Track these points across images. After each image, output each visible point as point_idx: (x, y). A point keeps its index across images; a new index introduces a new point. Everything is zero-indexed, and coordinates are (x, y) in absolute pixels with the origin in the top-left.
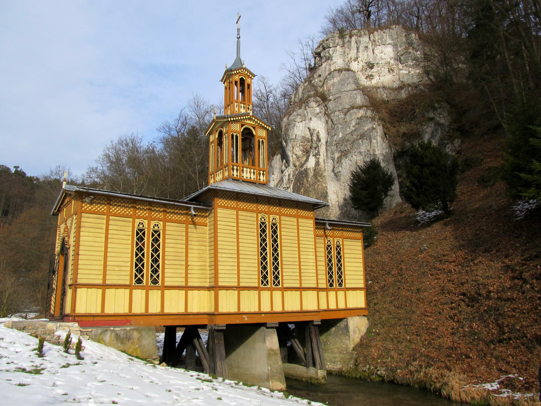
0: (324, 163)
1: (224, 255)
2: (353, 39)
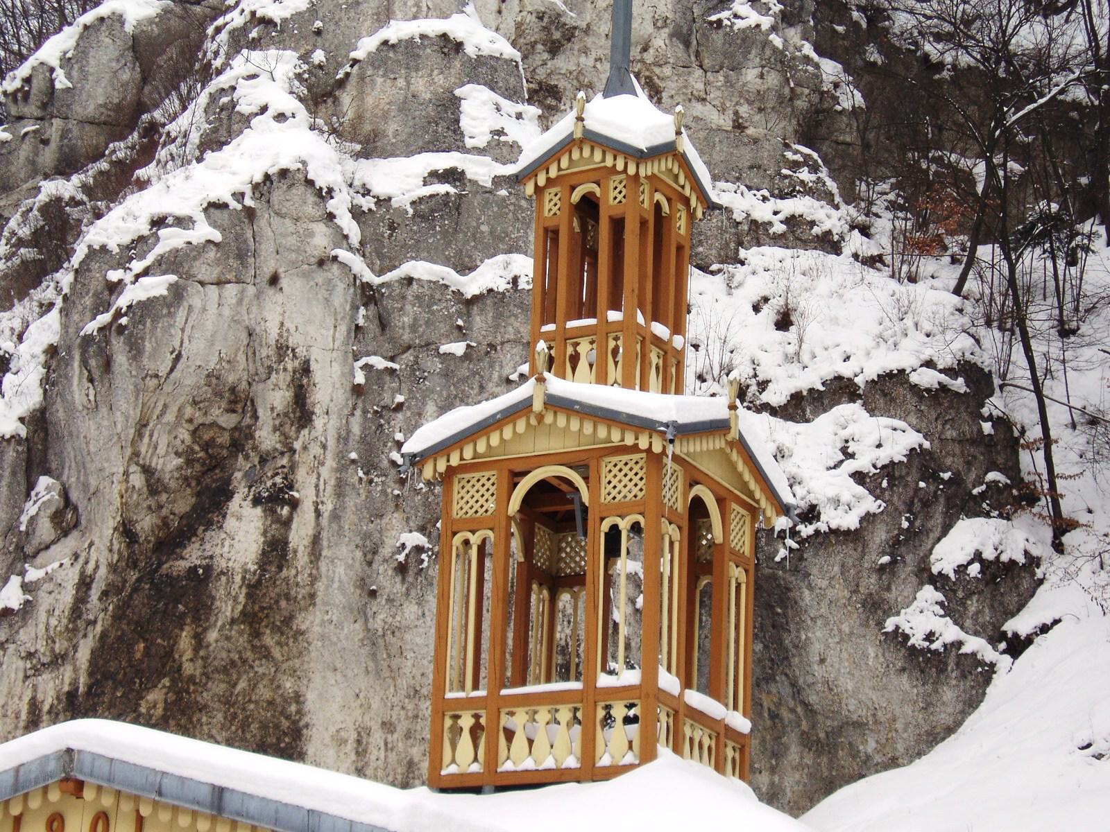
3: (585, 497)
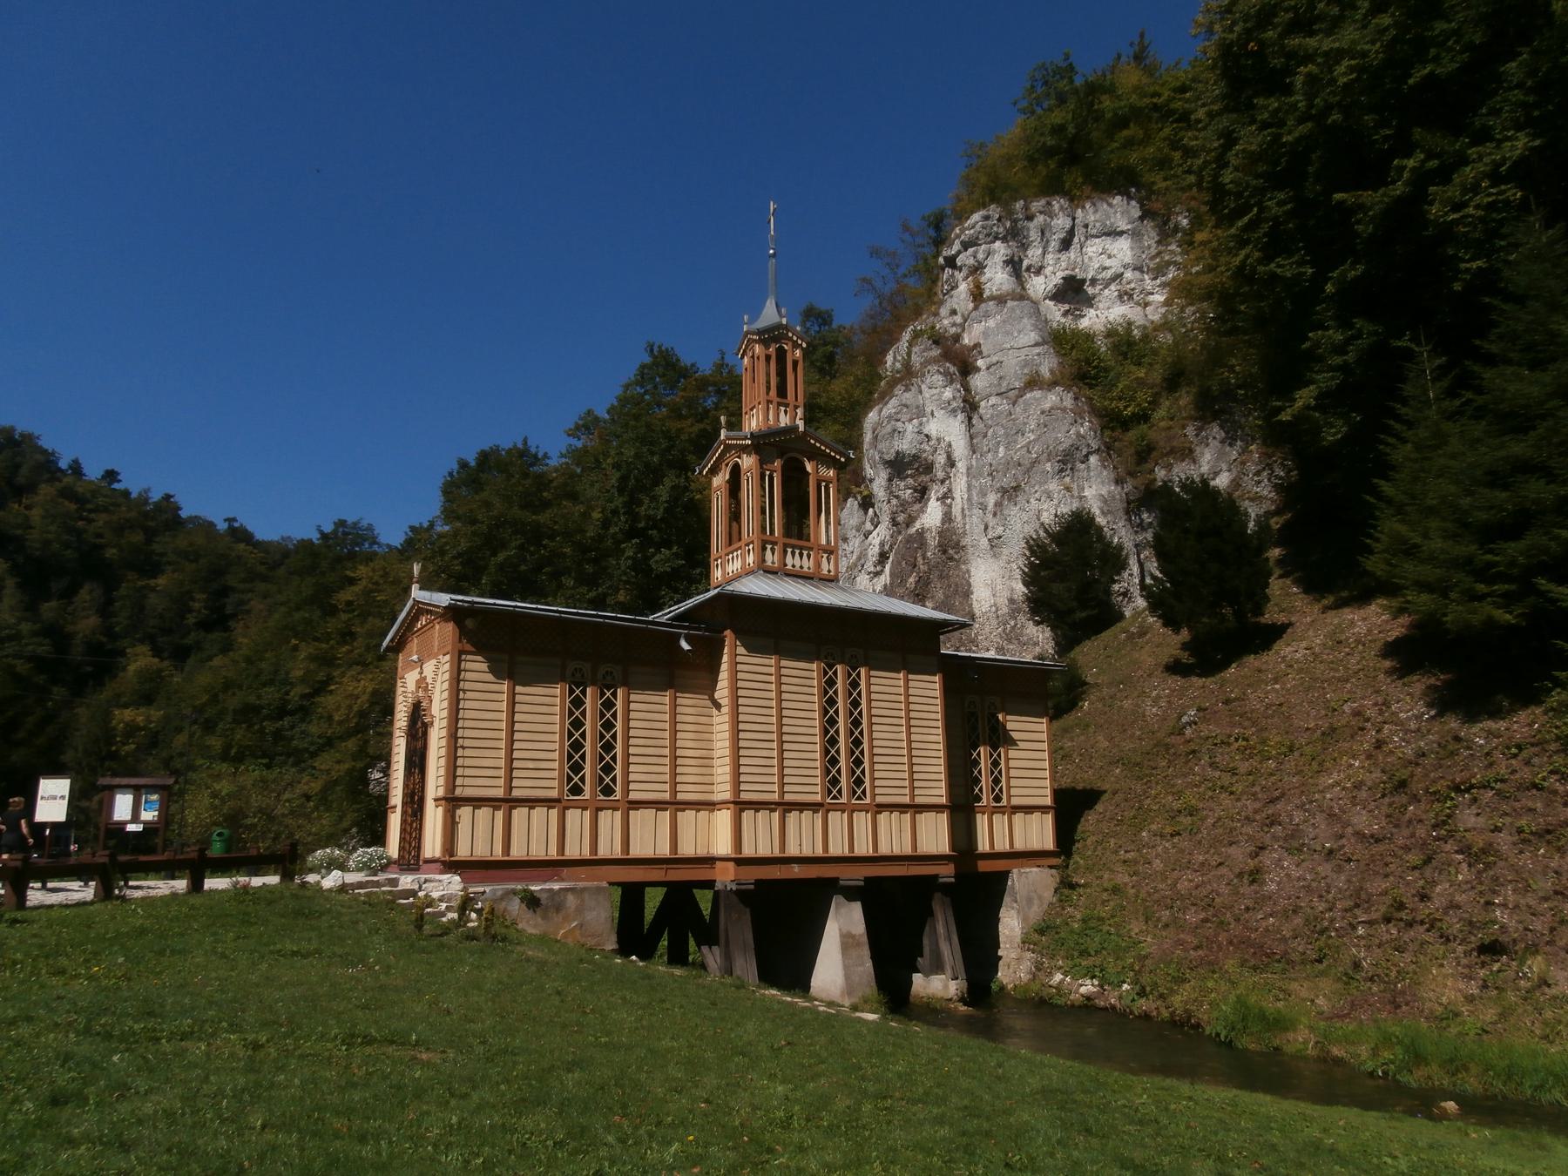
0: (964, 516)
1: (748, 735)
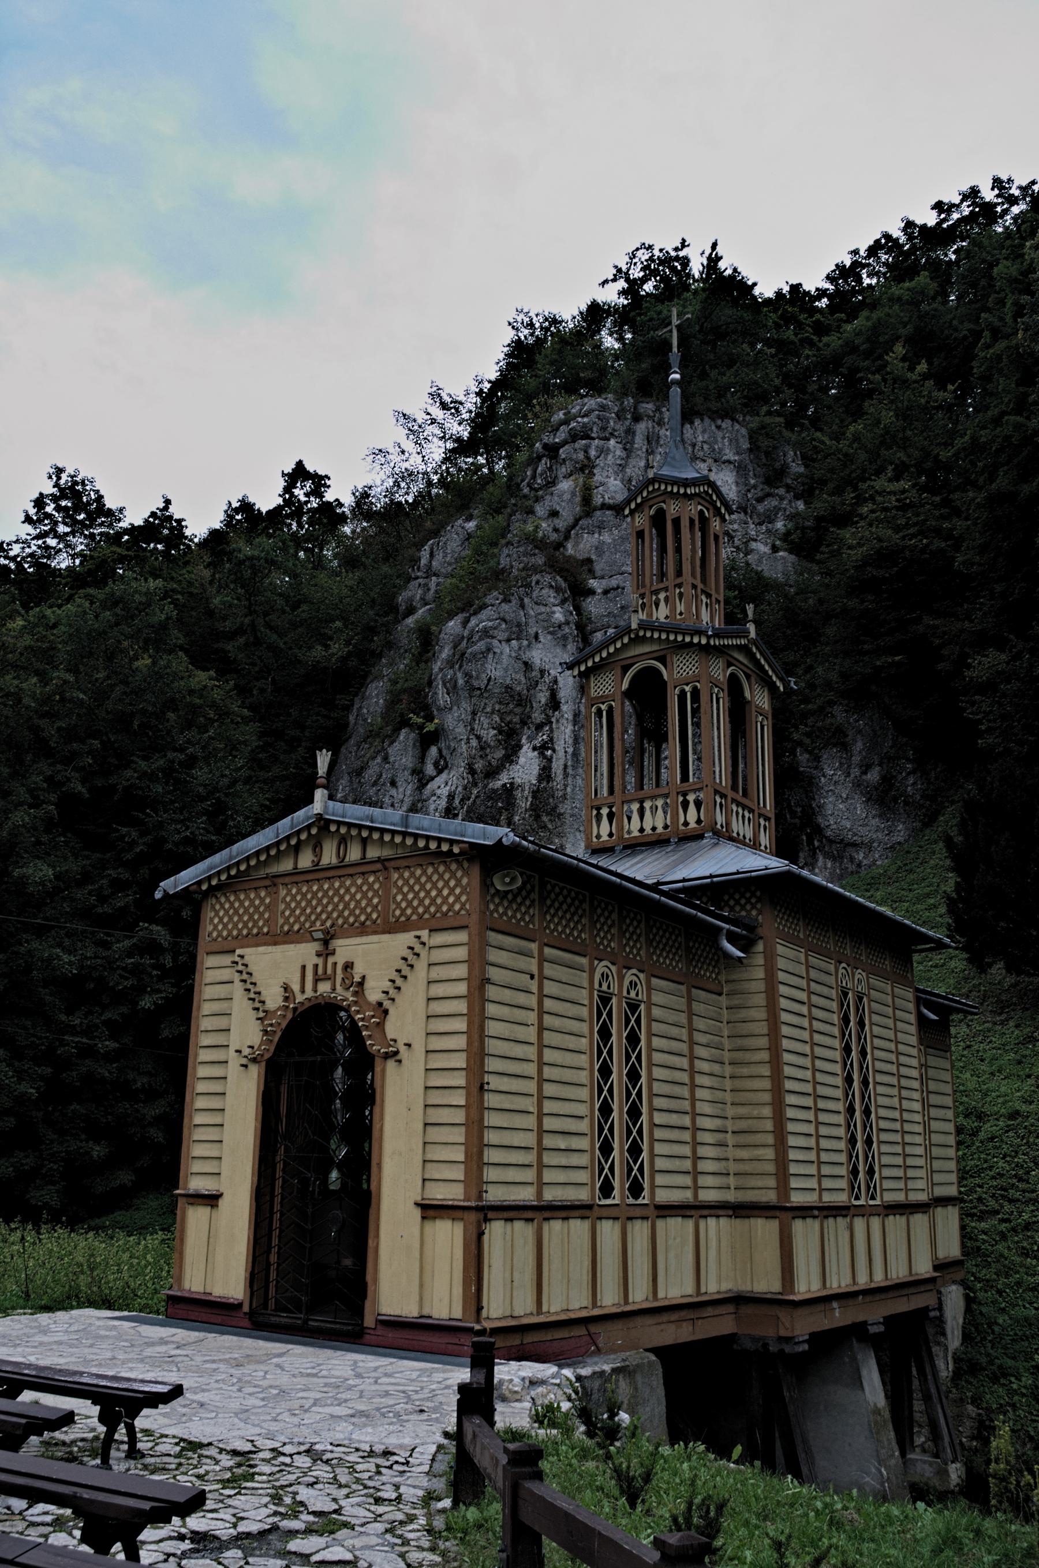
0: (566, 775)
2: (641, 428)
3: (666, 677)
